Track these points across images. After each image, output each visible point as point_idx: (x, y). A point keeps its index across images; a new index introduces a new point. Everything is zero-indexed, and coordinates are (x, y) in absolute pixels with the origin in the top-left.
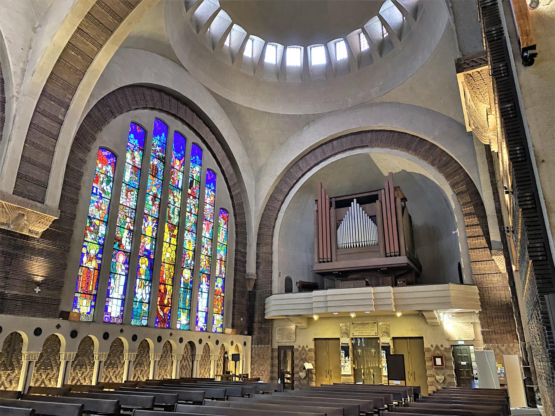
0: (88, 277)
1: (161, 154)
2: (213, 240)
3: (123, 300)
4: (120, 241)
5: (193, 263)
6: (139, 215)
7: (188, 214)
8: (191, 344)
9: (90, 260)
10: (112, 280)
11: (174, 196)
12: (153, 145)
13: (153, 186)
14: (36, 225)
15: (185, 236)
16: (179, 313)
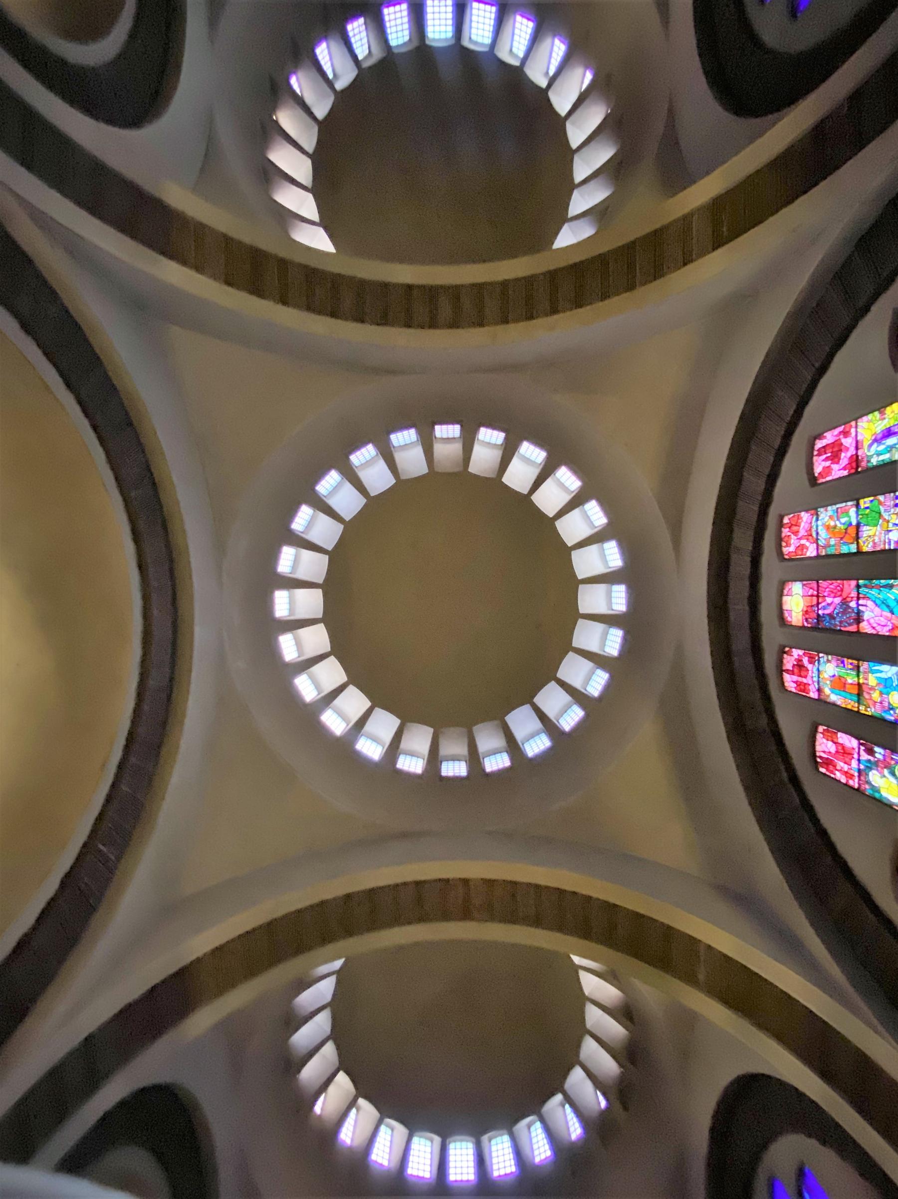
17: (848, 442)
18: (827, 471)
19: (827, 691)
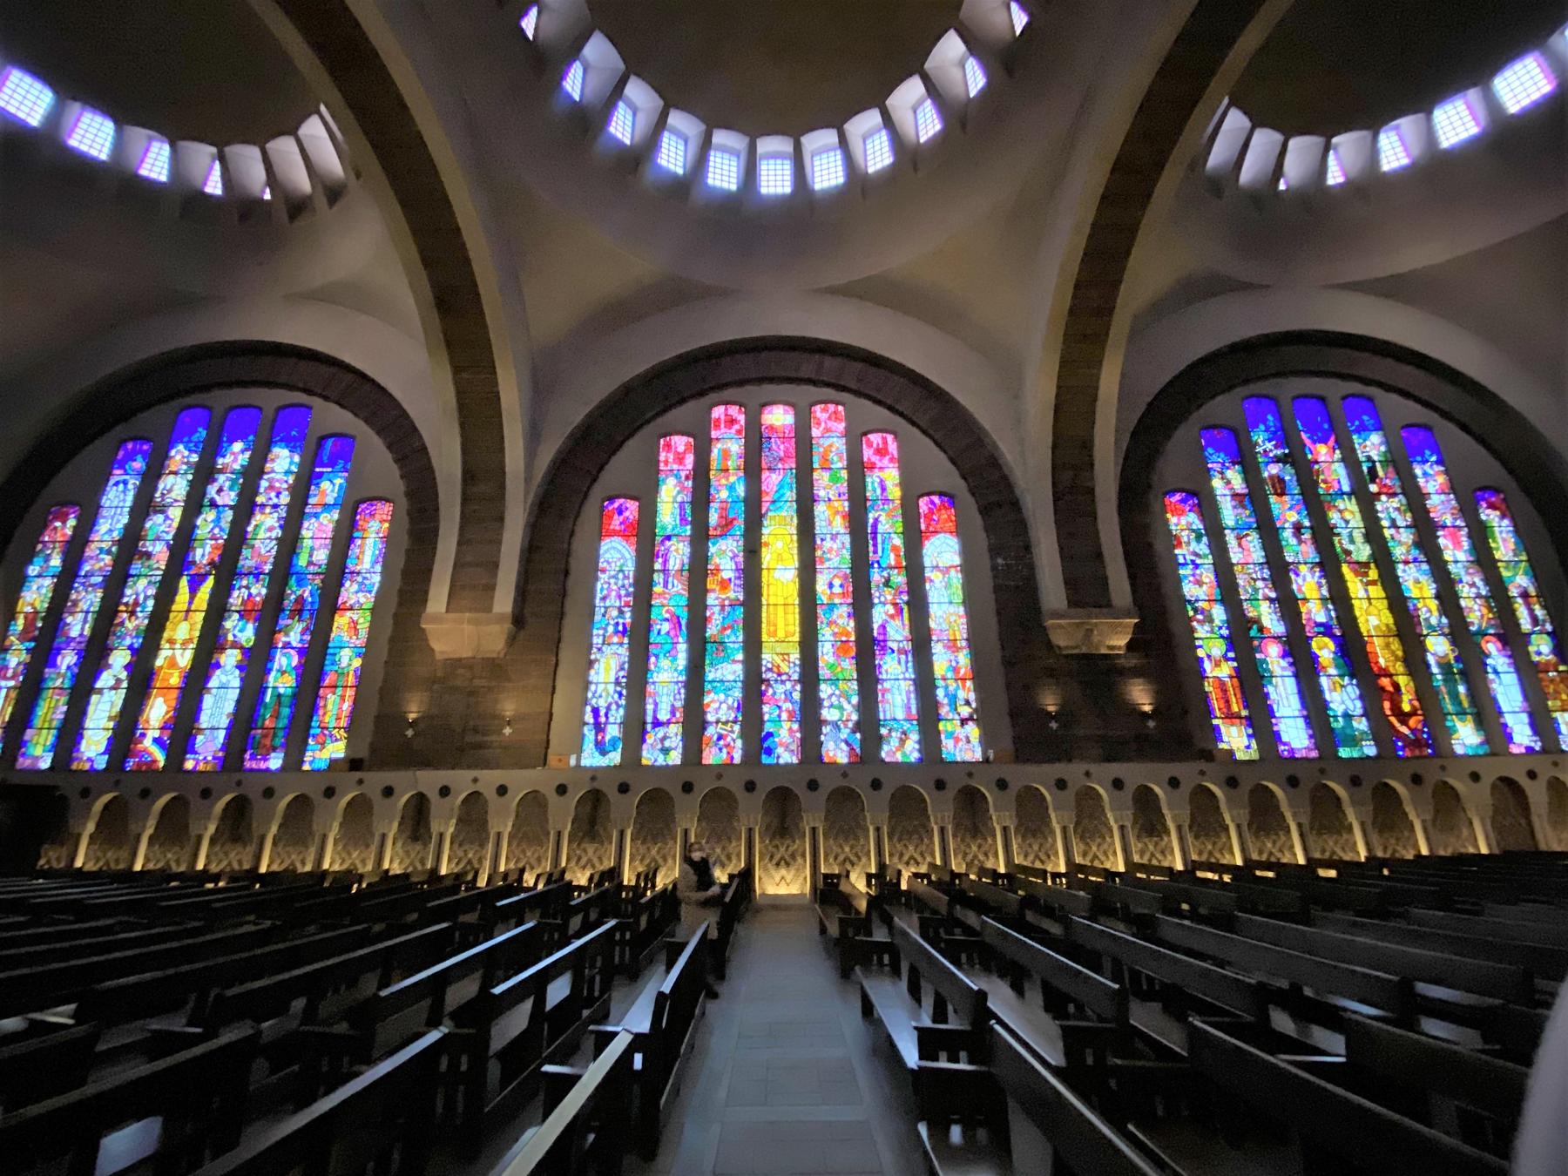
0: (1225, 691)
1: (1279, 452)
2: (1484, 559)
3: (1306, 718)
4: (1257, 621)
5: (1444, 620)
6: (1279, 570)
7: (1387, 533)
8: (1508, 782)
9: (1217, 664)
10: (1270, 689)
11: (1341, 512)
12: (1257, 444)
13: (1287, 512)
14: (1116, 639)
15: (1400, 573)
16: (1449, 724)
17: (886, 461)
18: (870, 445)
19: (719, 445)
